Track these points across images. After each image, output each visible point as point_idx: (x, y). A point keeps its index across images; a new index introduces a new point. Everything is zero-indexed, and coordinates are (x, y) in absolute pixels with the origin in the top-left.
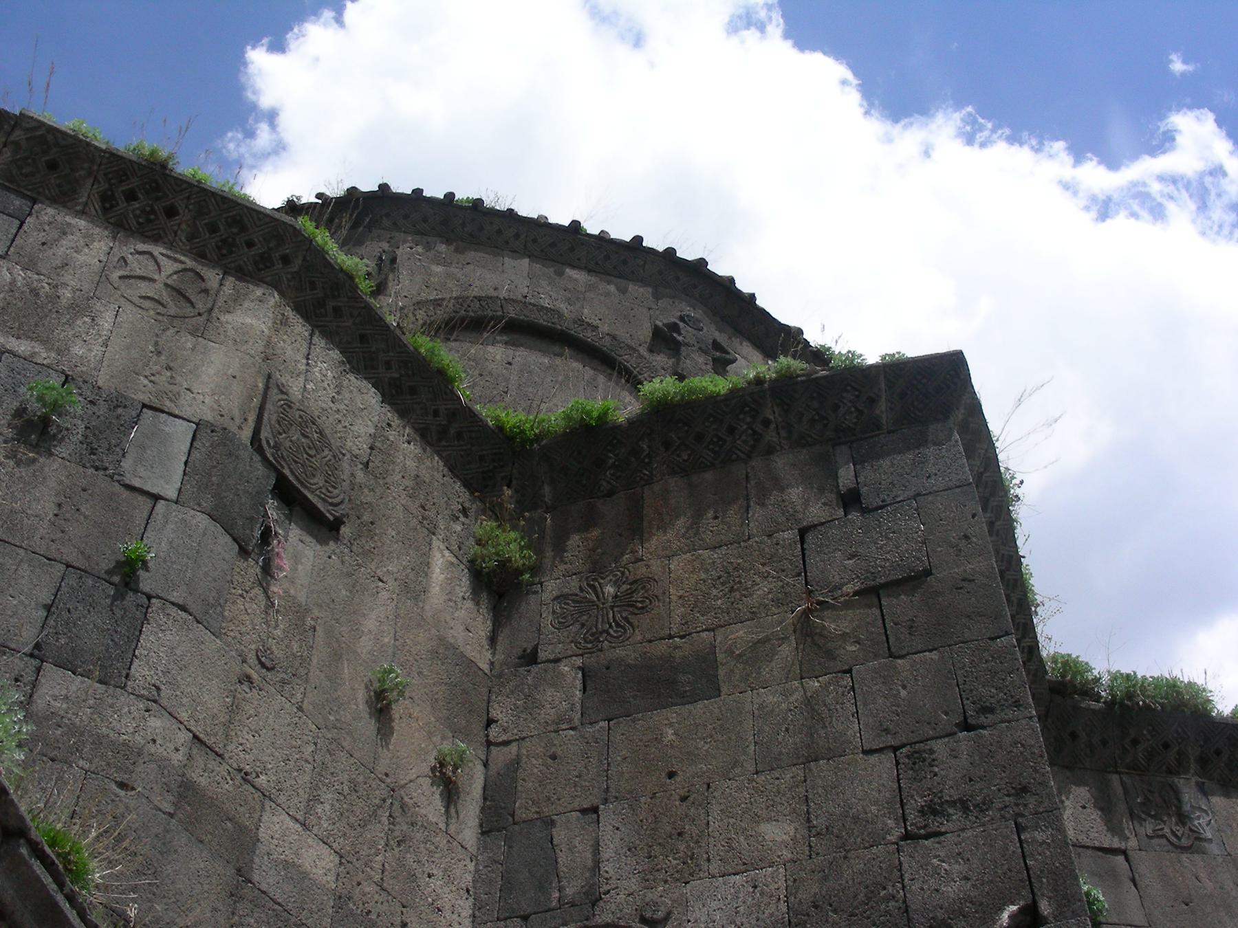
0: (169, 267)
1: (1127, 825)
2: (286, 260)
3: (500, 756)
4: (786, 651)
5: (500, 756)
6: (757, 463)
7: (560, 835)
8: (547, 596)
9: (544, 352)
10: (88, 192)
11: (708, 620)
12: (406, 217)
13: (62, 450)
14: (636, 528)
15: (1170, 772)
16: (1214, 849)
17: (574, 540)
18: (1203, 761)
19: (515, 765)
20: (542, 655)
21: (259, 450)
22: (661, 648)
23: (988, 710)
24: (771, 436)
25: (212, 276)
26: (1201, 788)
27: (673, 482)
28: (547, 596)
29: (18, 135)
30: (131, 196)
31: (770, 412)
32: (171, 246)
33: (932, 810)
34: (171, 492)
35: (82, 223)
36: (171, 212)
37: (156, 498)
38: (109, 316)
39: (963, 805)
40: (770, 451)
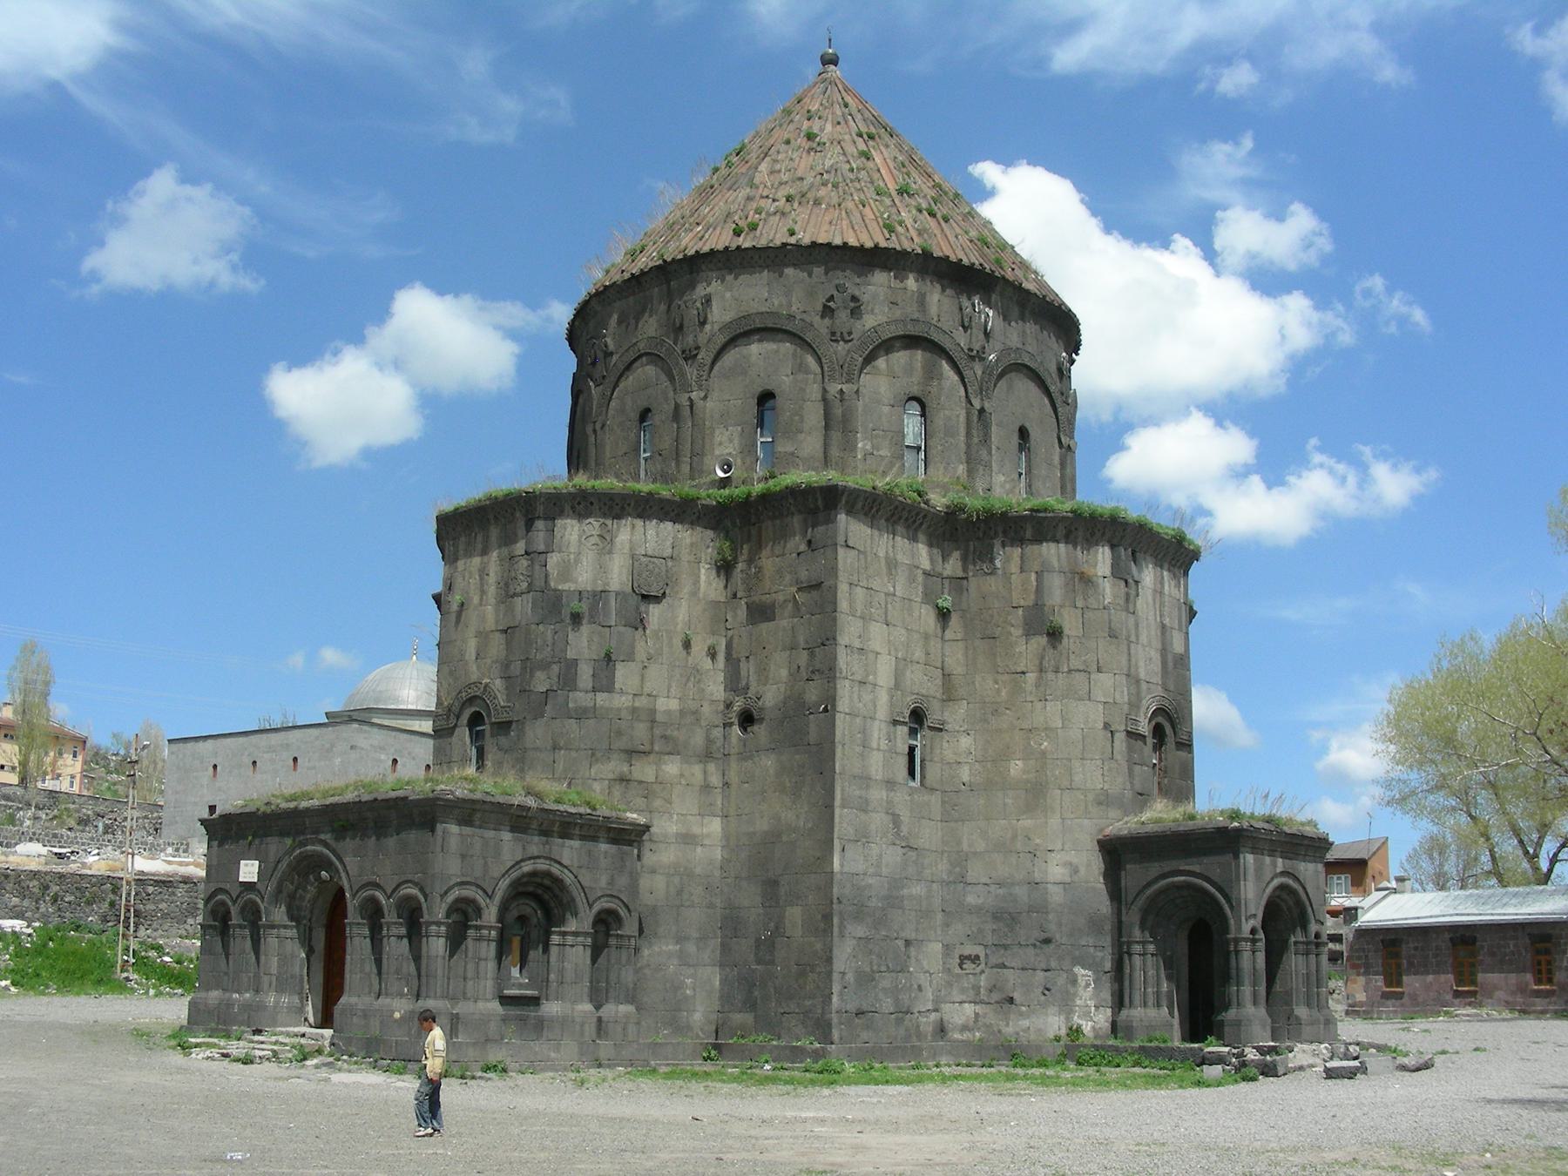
0: (596, 524)
1: (971, 567)
2: (629, 505)
3: (729, 636)
4: (790, 605)
5: (730, 633)
6: (789, 519)
7: (741, 664)
8: (739, 570)
9: (773, 341)
10: (567, 508)
11: (774, 589)
12: (711, 262)
13: (585, 621)
14: (760, 546)
15: (992, 538)
16: (1000, 572)
17: (745, 546)
18: (1004, 532)
19: (732, 637)
20: (738, 596)
21: (634, 591)
22: (764, 598)
23: (828, 639)
24: (792, 509)
25: (609, 522)
26: (1004, 546)
27: (770, 523)
28: (739, 570)
29: (542, 499)
30: (579, 503)
31: (791, 501)
32: (595, 517)
33: (813, 672)
34: (613, 624)
35: (569, 521)
36: (592, 503)
37: (610, 627)
38: (585, 559)
39: (818, 671)
40: (793, 514)
